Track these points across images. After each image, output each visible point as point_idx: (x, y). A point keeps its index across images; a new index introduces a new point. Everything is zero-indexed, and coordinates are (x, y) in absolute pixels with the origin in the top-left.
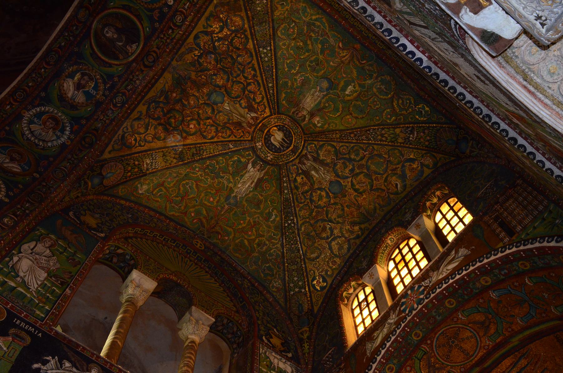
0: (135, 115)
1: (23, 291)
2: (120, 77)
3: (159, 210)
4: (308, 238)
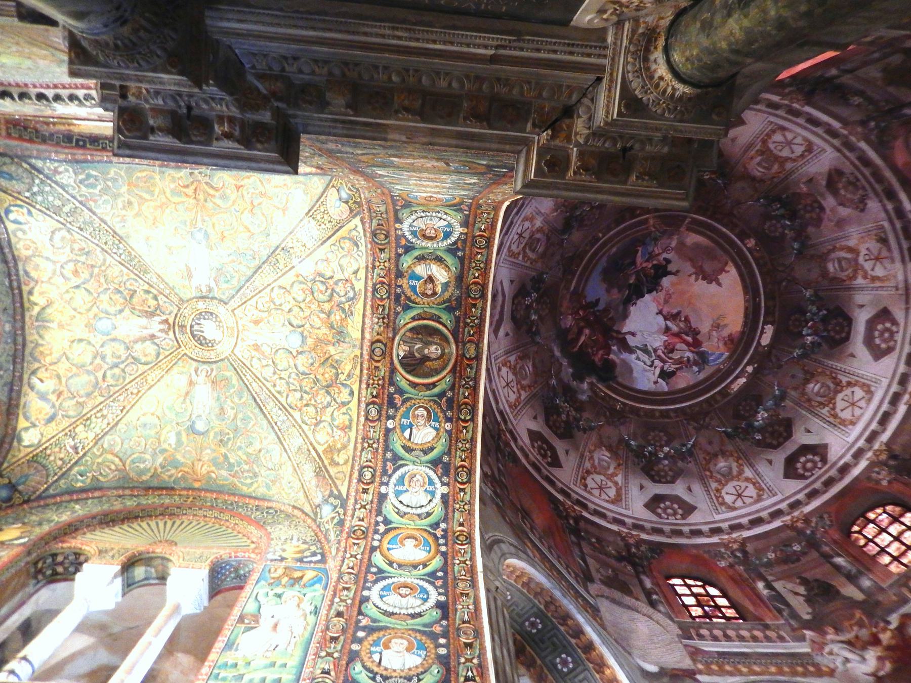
0: (362, 274)
2: (397, 314)
4: (84, 249)
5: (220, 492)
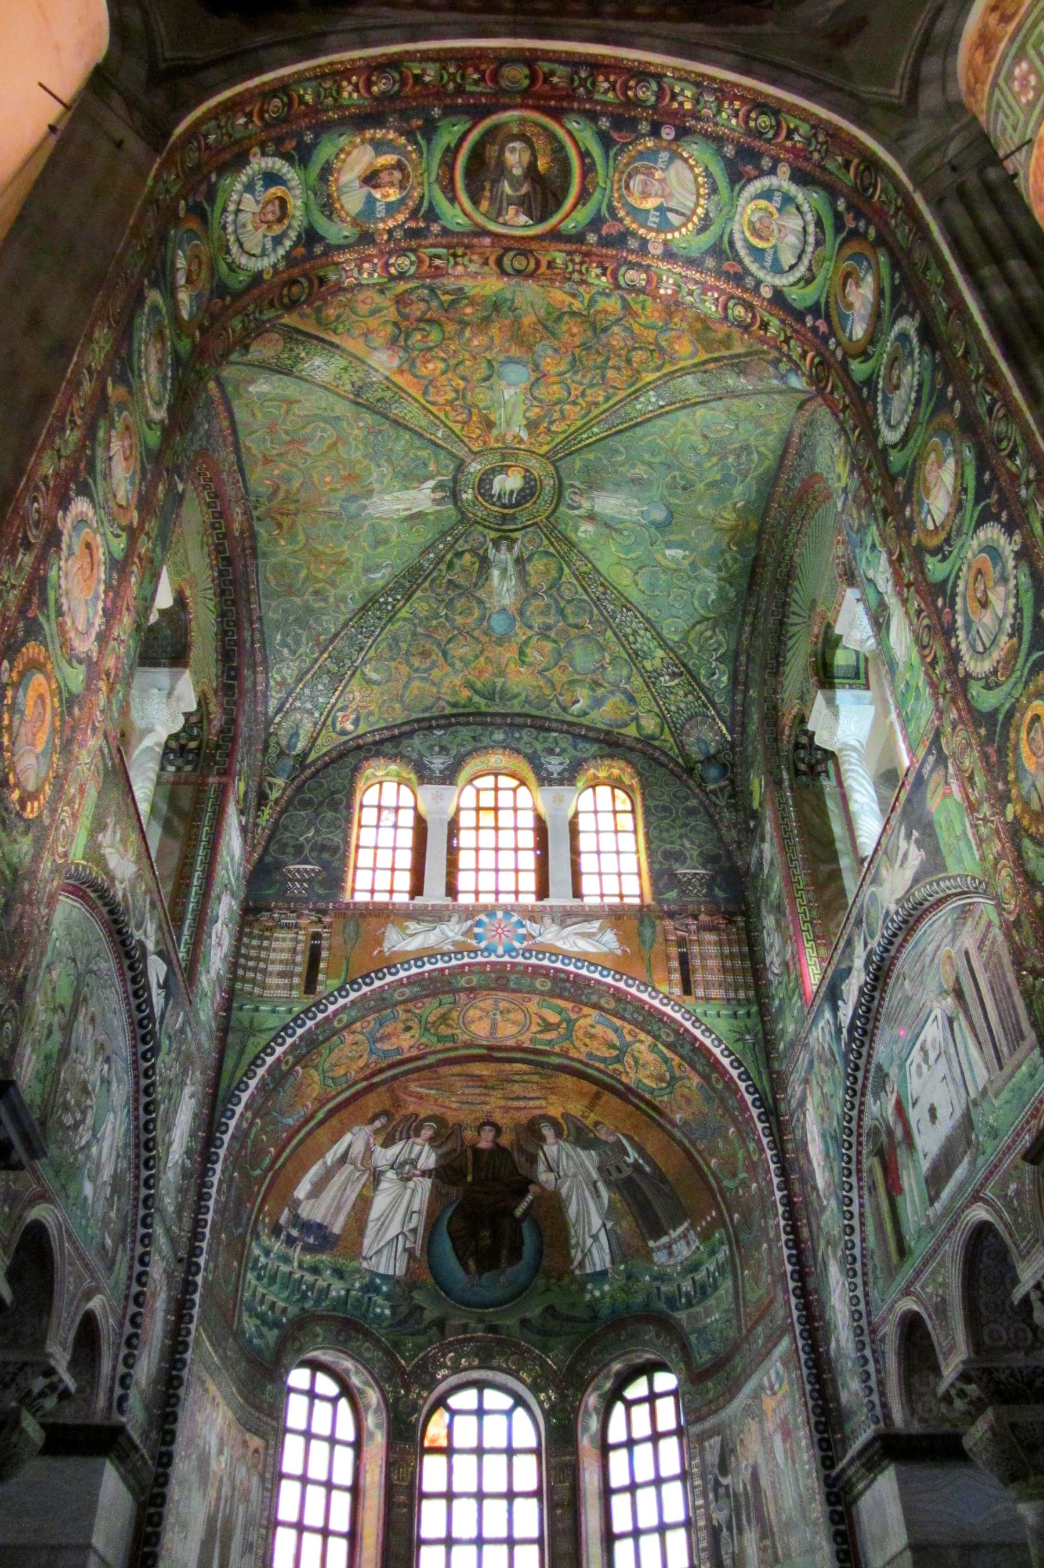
2: (445, 231)
3: (240, 428)
5: (770, 498)
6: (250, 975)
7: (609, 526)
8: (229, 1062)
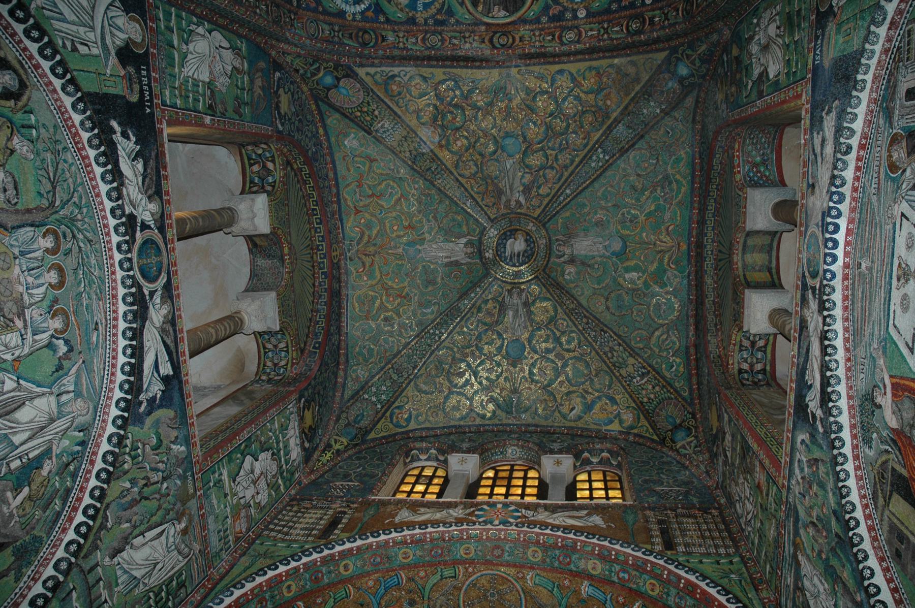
0: (426, 71)
1: (177, 59)
3: (340, 180)
6: (278, 528)
7: (584, 263)
8: (235, 571)
